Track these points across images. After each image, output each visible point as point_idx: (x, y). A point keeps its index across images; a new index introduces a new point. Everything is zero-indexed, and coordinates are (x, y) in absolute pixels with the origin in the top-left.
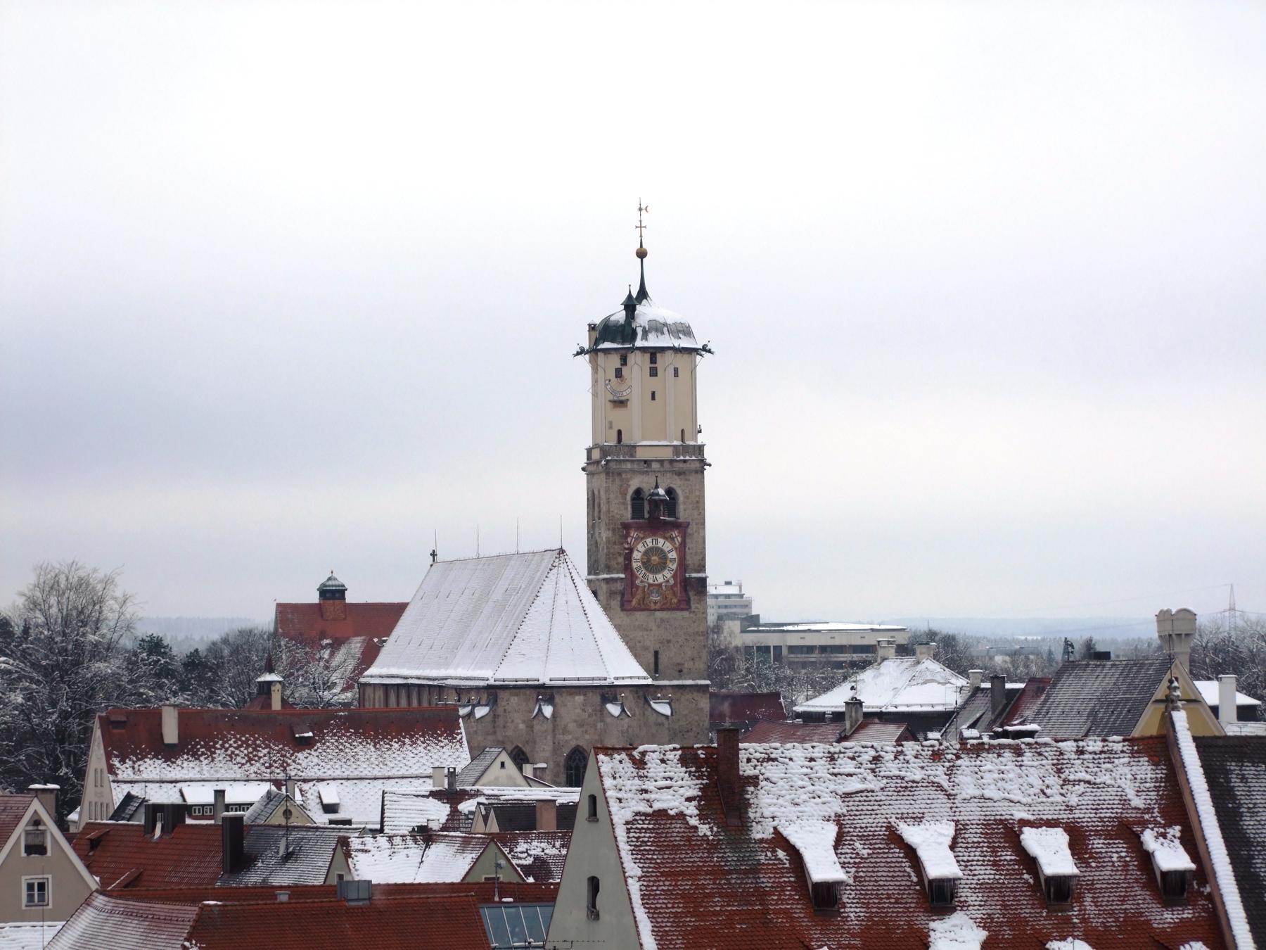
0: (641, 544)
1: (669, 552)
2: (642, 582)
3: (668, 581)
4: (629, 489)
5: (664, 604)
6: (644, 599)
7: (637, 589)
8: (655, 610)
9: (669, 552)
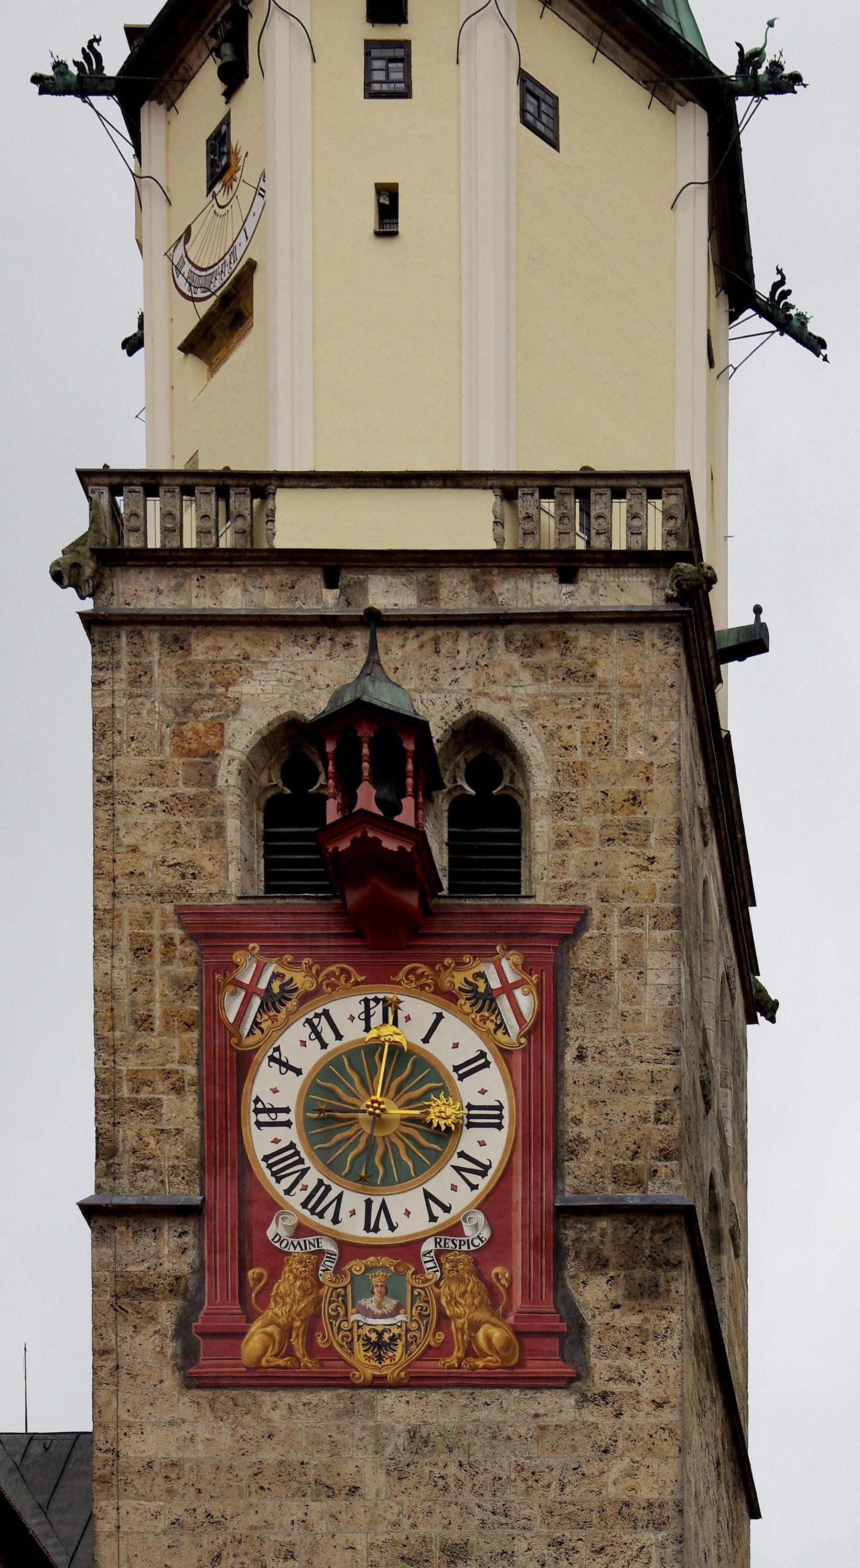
0: (299, 1030)
1: (465, 1070)
2: (301, 1230)
3: (455, 1230)
4: (232, 726)
5: (429, 1352)
6: (313, 1323)
7: (275, 1274)
8: (379, 1384)
9: (465, 1070)
